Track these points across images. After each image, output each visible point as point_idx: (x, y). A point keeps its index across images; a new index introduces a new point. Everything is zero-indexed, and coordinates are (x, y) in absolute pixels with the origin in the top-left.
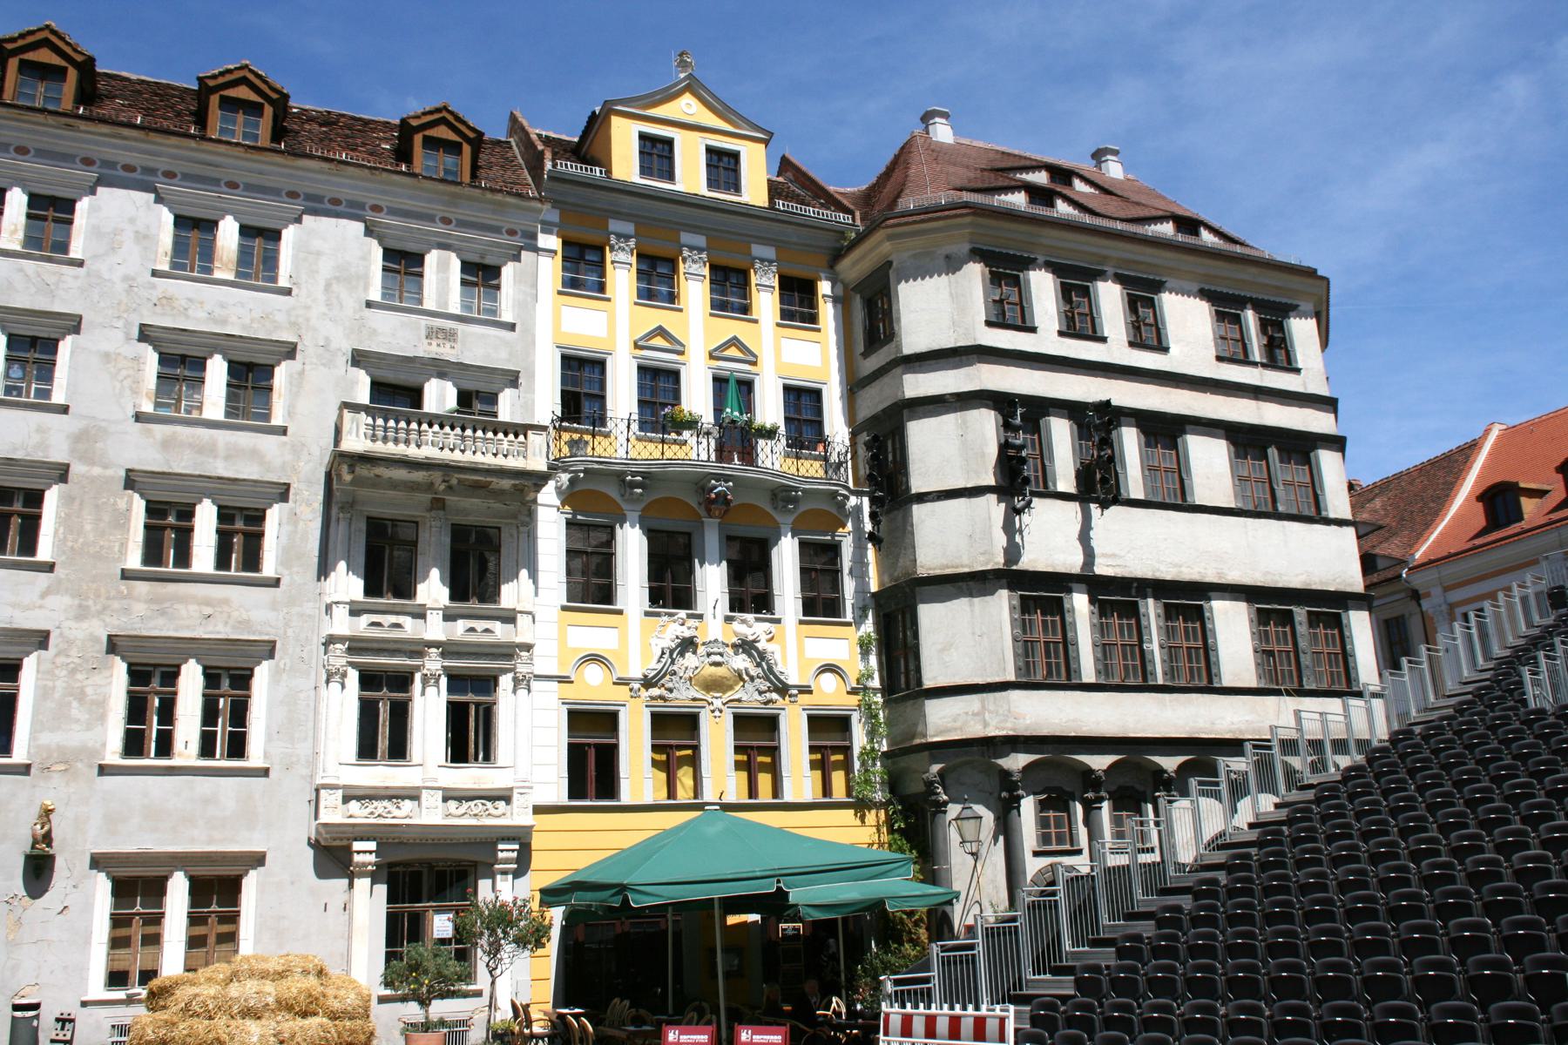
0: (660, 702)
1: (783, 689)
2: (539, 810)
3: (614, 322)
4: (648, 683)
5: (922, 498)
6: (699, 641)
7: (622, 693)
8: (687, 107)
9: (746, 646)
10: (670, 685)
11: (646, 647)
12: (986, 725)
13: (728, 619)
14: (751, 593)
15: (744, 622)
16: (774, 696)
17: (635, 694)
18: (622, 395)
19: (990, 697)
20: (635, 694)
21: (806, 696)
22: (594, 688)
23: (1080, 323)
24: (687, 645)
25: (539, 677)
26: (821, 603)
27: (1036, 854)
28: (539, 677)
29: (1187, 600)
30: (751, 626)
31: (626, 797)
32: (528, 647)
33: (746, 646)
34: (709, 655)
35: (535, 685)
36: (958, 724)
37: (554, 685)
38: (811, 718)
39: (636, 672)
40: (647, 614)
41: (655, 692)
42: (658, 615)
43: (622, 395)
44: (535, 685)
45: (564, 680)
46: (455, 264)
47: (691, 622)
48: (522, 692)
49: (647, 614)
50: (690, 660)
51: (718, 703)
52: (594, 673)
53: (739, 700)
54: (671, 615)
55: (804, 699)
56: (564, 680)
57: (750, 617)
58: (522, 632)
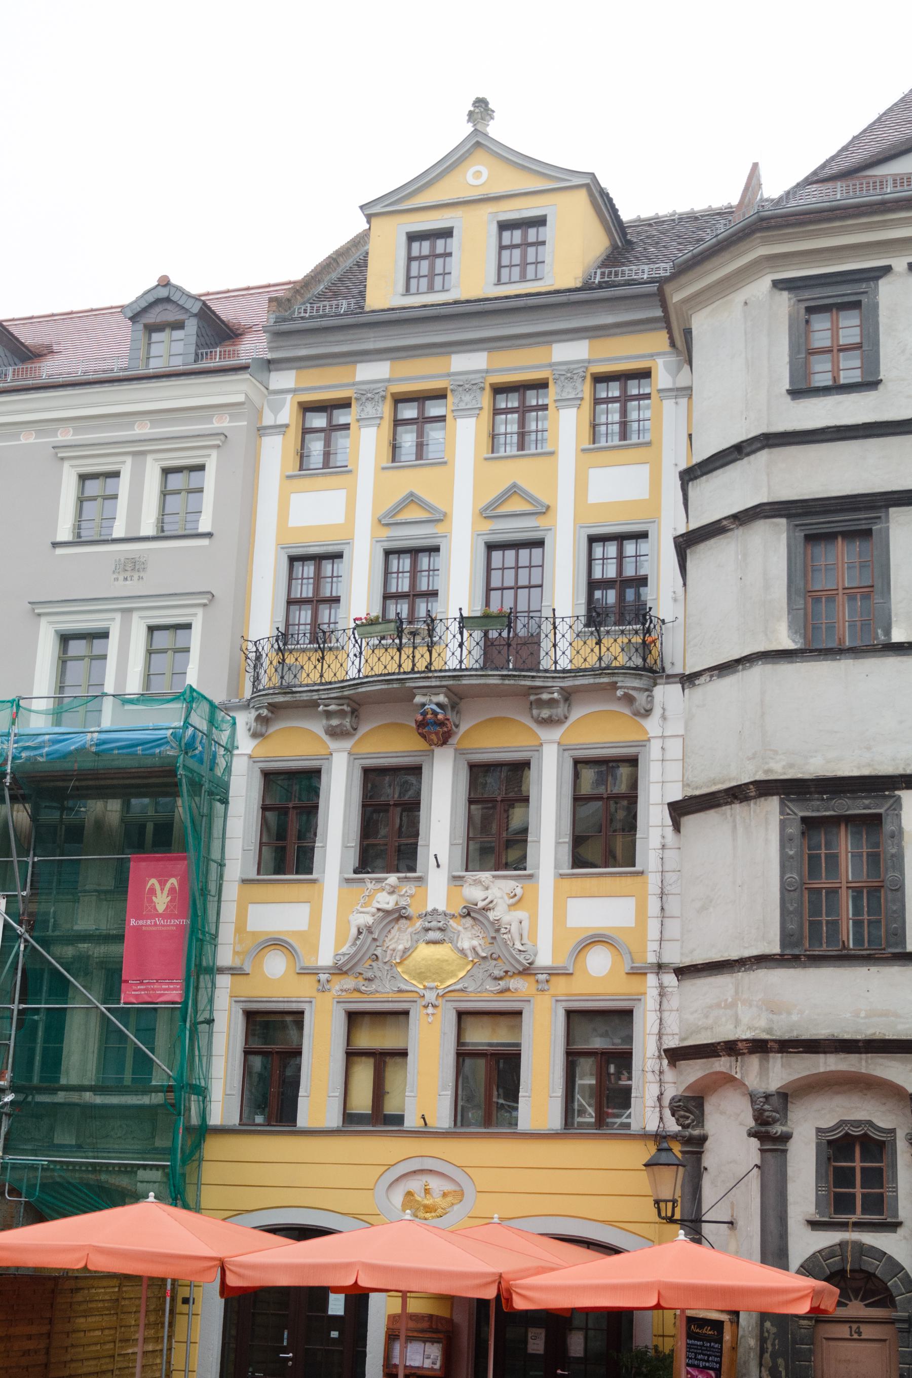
0: (356, 995)
1: (527, 971)
4: (339, 970)
10: (369, 974)
11: (342, 923)
12: (737, 1022)
15: (478, 882)
18: (359, 592)
19: (745, 978)
21: (562, 980)
24: (398, 915)
27: (814, 1225)
30: (492, 888)
31: (303, 1121)
34: (427, 930)
36: (710, 1021)
39: (326, 958)
40: (348, 880)
41: (349, 982)
42: (362, 881)
43: (359, 592)
47: (409, 888)
50: (399, 939)
51: (430, 996)
54: (379, 880)
55: (560, 986)
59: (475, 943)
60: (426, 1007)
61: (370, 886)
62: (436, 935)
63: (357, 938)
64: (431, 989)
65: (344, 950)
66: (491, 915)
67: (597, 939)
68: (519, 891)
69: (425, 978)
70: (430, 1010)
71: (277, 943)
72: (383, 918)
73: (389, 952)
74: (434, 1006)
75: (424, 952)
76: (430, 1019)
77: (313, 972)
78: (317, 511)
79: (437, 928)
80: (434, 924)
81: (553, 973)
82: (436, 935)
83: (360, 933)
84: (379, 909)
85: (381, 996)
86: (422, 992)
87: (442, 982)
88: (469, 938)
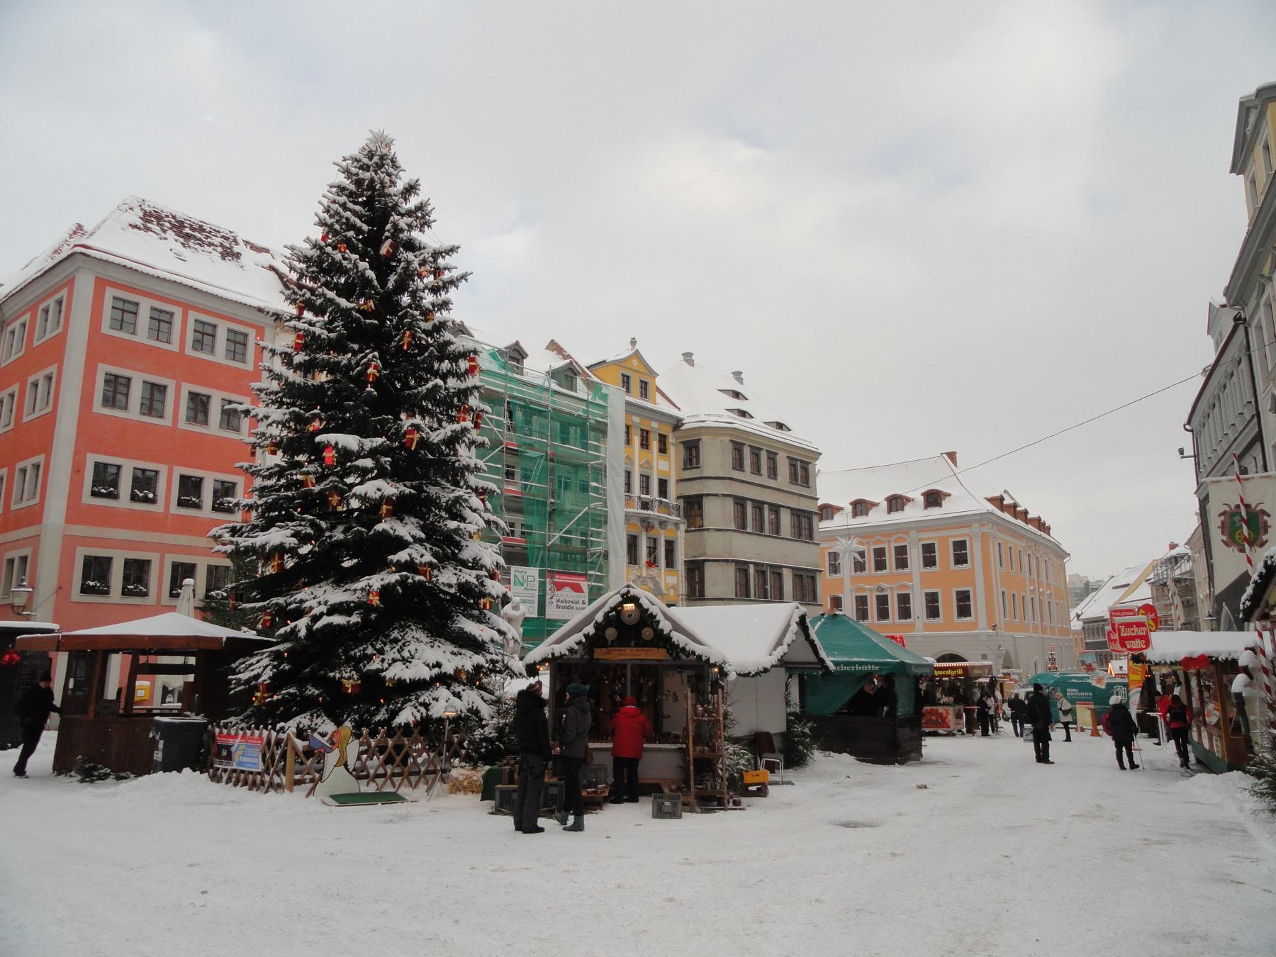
23: (757, 470)
26: (670, 563)
29: (777, 571)
30: (653, 572)
33: (652, 578)
67: (674, 587)
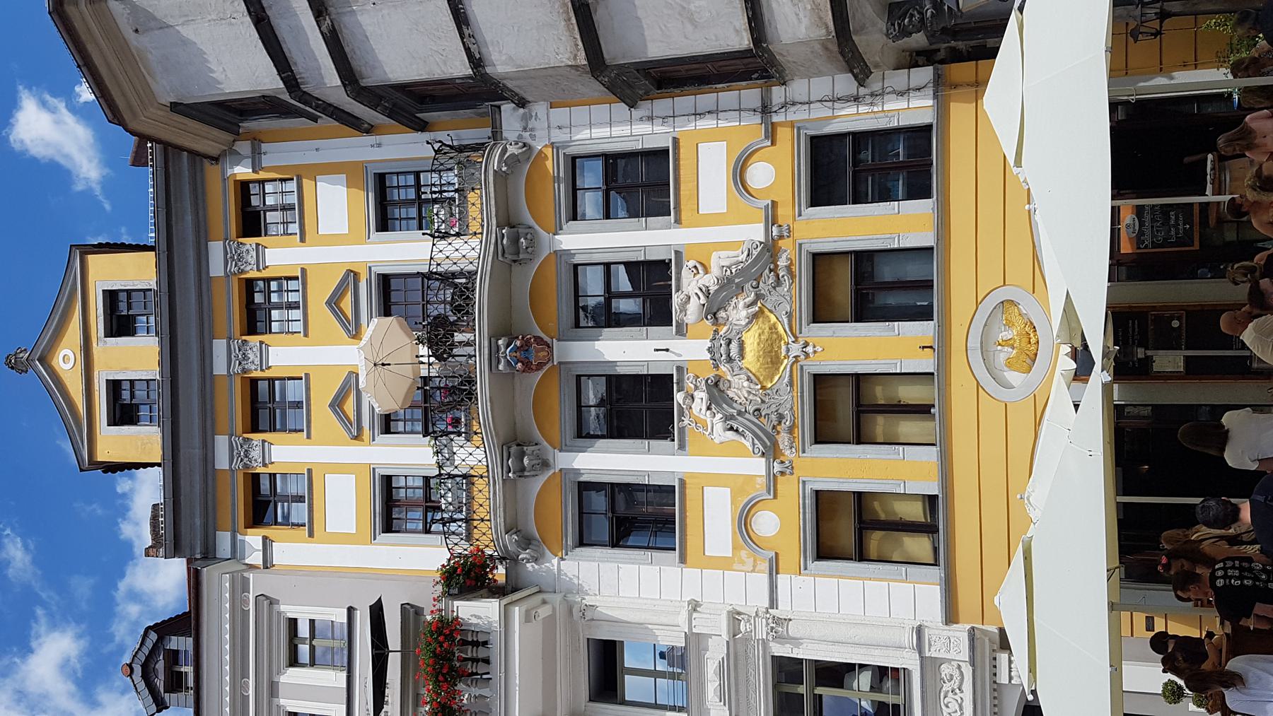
0: (798, 432)
1: (770, 249)
2: (951, 616)
3: (333, 465)
4: (771, 451)
5: (476, 62)
6: (711, 375)
7: (788, 487)
8: (66, 360)
9: (713, 309)
11: (724, 450)
13: (681, 331)
14: (649, 292)
16: (782, 262)
17: (789, 469)
20: (789, 469)
21: (780, 211)
22: (781, 523)
24: (716, 390)
25: (773, 603)
28: (773, 603)
30: (689, 291)
32: (735, 617)
34: (730, 360)
35: (783, 610)
37: (782, 580)
38: (815, 201)
39: (757, 466)
40: (682, 446)
41: (783, 439)
42: (682, 430)
44: (783, 610)
45: (774, 569)
46: (292, 676)
48: (793, 630)
49: (682, 446)
50: (739, 388)
51: (796, 349)
52: (766, 523)
53: (789, 315)
54: (681, 413)
55: (785, 213)
56: (774, 569)
57: (676, 299)
58: (715, 627)
59: (741, 304)
60: (807, 355)
61: (686, 422)
62: (734, 347)
63: (737, 431)
64: (788, 350)
65: (748, 444)
66: (713, 289)
68: (691, 263)
69: (778, 357)
70: (810, 349)
71: (744, 522)
72: (718, 405)
73: (751, 397)
74: (806, 345)
75: (751, 359)
76: (819, 349)
77: (772, 482)
78: (344, 503)
79: (726, 350)
80: (723, 350)
81: (771, 217)
82: (734, 347)
83: (731, 429)
84: (709, 408)
85: (796, 404)
86: (791, 359)
87: (780, 338)
88: (738, 312)
